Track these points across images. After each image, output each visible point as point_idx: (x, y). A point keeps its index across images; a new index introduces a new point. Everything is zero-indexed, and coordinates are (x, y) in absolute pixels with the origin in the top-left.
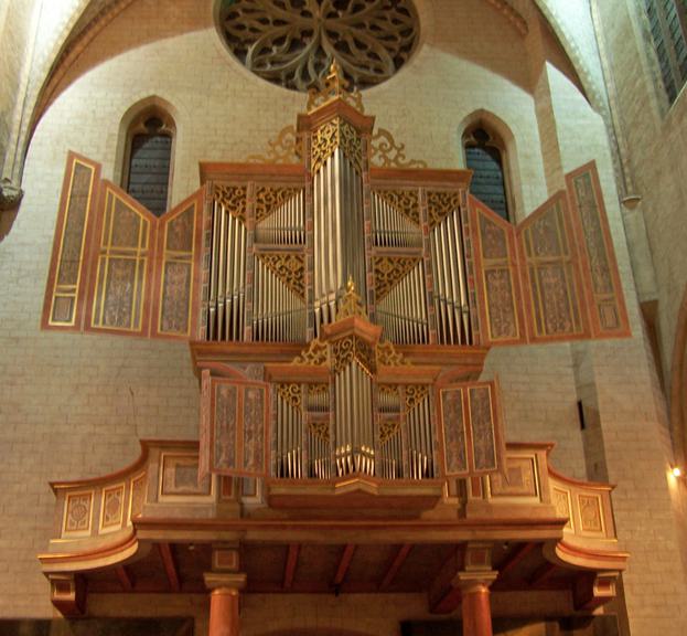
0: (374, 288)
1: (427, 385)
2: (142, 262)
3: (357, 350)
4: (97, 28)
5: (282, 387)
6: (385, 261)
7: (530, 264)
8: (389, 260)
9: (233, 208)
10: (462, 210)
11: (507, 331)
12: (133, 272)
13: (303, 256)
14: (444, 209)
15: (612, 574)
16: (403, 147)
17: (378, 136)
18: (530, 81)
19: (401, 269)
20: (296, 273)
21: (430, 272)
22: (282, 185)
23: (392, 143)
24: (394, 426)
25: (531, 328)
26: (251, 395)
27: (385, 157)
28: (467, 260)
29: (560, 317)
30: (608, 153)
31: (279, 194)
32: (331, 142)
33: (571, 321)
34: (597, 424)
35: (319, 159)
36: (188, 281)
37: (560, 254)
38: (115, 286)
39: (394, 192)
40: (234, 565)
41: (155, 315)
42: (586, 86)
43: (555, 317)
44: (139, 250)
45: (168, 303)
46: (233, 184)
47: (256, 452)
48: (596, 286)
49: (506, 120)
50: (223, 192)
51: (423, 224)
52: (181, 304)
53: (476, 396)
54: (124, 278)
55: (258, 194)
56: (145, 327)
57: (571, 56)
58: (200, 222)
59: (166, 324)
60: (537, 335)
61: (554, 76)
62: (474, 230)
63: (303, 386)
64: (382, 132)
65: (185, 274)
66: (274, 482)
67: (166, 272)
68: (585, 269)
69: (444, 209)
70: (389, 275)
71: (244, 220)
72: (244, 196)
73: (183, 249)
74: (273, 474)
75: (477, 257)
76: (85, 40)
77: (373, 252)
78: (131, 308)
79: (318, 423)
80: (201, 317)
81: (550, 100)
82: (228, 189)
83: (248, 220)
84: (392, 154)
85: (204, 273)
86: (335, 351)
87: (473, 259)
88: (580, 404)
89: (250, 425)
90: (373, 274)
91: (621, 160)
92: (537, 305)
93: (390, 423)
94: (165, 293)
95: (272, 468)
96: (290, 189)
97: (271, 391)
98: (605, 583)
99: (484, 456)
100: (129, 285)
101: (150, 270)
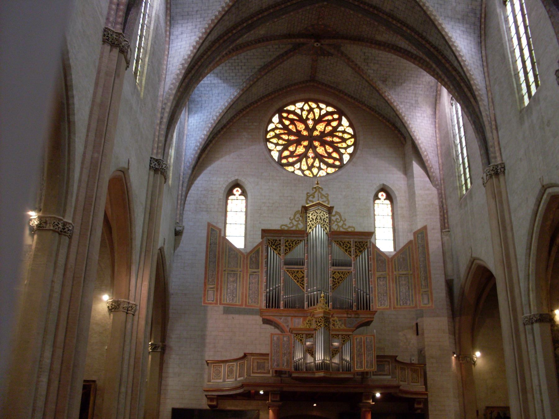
0: (332, 285)
1: (350, 335)
2: (240, 274)
3: (324, 323)
4: (211, 145)
5: (296, 335)
6: (337, 273)
7: (395, 275)
8: (338, 272)
9: (275, 250)
10: (369, 249)
11: (384, 304)
12: (237, 279)
13: (304, 271)
14: (362, 249)
15: (422, 400)
16: (345, 220)
17: (334, 216)
18: (407, 170)
19: (343, 276)
20: (301, 278)
23: (341, 219)
24: (337, 351)
25: (394, 303)
26: (285, 339)
27: (338, 226)
28: (370, 272)
29: (406, 299)
30: (438, 207)
31: (294, 243)
32: (316, 221)
33: (410, 301)
34: (423, 334)
35: (310, 228)
36: (258, 282)
37: (408, 271)
38: (230, 285)
39: (341, 241)
40: (278, 399)
41: (246, 297)
42: (430, 174)
43: (404, 299)
44: (239, 270)
45: (251, 292)
46: (276, 238)
47: (287, 361)
48: (422, 285)
49: (393, 189)
50: (271, 242)
51: (353, 256)
52: (256, 292)
53: (368, 340)
54: (233, 282)
55: (285, 243)
56: (242, 302)
57: (424, 159)
58: (262, 256)
59: (250, 301)
60: (396, 307)
61: (416, 168)
62: (374, 259)
63: (304, 335)
66: (293, 372)
67: (250, 279)
69: (362, 249)
70: (338, 279)
71: (280, 255)
72: (280, 244)
73: (256, 269)
74: (293, 369)
75: (374, 270)
76: (206, 152)
78: (236, 294)
79: (310, 349)
80: (264, 298)
81: (413, 181)
82: (273, 240)
83: (282, 255)
84: (340, 224)
86: (316, 322)
87: (372, 272)
88: (417, 324)
89: (285, 350)
90: (331, 279)
91: (444, 211)
92: (397, 293)
93: (336, 350)
94: (249, 287)
95: (293, 366)
96: (298, 241)
97: (292, 337)
98: (419, 403)
99: (369, 364)
100: (235, 285)
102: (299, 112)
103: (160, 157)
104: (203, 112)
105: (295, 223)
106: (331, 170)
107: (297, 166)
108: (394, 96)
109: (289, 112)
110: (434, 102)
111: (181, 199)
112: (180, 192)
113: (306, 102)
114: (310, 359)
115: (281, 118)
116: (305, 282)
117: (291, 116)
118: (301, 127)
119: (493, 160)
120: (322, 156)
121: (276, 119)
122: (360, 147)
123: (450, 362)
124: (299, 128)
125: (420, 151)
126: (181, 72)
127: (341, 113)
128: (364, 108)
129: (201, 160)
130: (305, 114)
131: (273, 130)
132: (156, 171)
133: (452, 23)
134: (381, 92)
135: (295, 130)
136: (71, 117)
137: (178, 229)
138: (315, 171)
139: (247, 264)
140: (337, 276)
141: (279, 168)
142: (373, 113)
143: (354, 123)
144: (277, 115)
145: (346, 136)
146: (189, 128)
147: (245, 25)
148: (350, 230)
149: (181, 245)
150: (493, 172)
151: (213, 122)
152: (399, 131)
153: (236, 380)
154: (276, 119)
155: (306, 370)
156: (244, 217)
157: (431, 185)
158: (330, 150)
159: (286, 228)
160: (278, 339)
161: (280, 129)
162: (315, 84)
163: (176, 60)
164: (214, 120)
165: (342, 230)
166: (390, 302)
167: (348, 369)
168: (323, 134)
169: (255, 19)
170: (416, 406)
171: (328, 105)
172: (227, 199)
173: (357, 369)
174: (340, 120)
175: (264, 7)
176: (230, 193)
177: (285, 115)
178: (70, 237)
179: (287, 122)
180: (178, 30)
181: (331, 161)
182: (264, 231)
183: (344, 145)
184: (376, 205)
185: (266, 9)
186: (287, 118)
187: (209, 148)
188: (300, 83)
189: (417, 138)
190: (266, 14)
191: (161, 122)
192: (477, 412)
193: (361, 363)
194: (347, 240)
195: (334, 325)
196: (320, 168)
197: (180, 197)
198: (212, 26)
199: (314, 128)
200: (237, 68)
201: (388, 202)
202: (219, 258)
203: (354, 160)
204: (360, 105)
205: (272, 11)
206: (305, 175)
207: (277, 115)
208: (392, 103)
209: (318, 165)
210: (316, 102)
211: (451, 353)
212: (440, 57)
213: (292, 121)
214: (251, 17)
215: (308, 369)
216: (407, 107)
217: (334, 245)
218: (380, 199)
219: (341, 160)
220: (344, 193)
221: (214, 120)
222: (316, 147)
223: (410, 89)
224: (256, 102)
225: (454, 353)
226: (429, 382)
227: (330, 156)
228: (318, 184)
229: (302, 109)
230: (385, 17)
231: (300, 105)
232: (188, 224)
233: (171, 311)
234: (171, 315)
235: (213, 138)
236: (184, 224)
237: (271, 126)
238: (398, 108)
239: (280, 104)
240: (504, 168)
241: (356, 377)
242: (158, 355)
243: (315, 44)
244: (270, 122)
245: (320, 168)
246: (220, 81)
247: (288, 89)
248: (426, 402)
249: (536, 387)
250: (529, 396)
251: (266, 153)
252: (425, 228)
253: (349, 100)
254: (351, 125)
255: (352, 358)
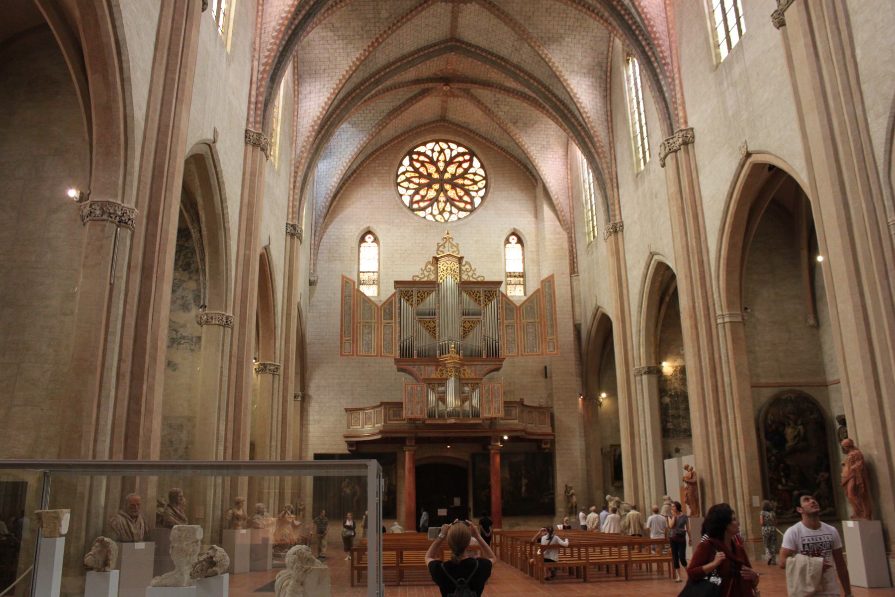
4: (342, 192)
9: (408, 300)
11: (512, 351)
17: (464, 266)
18: (537, 213)
21: (484, 326)
22: (426, 289)
26: (418, 388)
30: (567, 252)
34: (551, 377)
40: (413, 444)
42: (561, 218)
46: (408, 289)
49: (524, 233)
51: (482, 305)
58: (395, 307)
61: (547, 211)
62: (502, 308)
64: (467, 263)
65: (390, 330)
68: (545, 326)
74: (426, 417)
76: (337, 199)
77: (462, 318)
80: (398, 348)
84: (470, 274)
85: (398, 329)
98: (546, 443)
101: (378, 329)
102: (429, 153)
103: (295, 222)
104: (333, 157)
105: (426, 274)
106: (462, 214)
107: (429, 210)
108: (525, 138)
109: (419, 154)
110: (566, 142)
111: (314, 249)
112: (313, 242)
113: (437, 142)
114: (442, 407)
115: (411, 160)
116: (437, 331)
117: (422, 158)
118: (432, 169)
119: (612, 218)
120: (453, 200)
121: (406, 161)
122: (491, 190)
123: (577, 404)
124: (429, 171)
125: (551, 194)
126: (311, 135)
127: (472, 154)
128: (496, 148)
129: (332, 207)
130: (435, 155)
131: (404, 173)
132: (292, 235)
133: (578, 78)
134: (511, 134)
135: (425, 173)
136: (226, 225)
137: (312, 279)
138: (446, 215)
139: (381, 316)
140: (467, 325)
141: (409, 213)
142: (504, 154)
143: (485, 164)
144: (407, 158)
145: (477, 178)
146: (319, 174)
147: (372, 80)
148: (479, 279)
149: (316, 295)
150: (612, 230)
151: (342, 168)
152: (531, 173)
153: (374, 426)
154: (406, 161)
155: (439, 417)
156: (377, 264)
157: (561, 229)
158: (461, 193)
159: (418, 279)
160: (412, 388)
161: (411, 172)
162: (446, 124)
163: (305, 121)
164: (344, 166)
165: (472, 279)
166: (518, 350)
167: (476, 415)
168: (454, 176)
169: (382, 73)
170: (543, 446)
171: (459, 145)
172: (359, 246)
173: (486, 414)
174: (471, 160)
175: (391, 61)
176: (362, 240)
177: (415, 157)
178: (232, 329)
179: (417, 165)
180: (306, 89)
181: (462, 205)
182: (396, 283)
183: (476, 188)
184: (506, 249)
185: (393, 63)
186: (417, 161)
187: (339, 195)
188: (430, 123)
189: (548, 181)
190: (393, 67)
191: (294, 187)
192: (602, 449)
193: (489, 410)
194: (476, 290)
195: (464, 374)
196: (451, 213)
197: (312, 247)
198: (340, 86)
199: (445, 171)
200: (365, 112)
201: (519, 246)
202: (354, 311)
203: (485, 204)
204: (492, 146)
205: (399, 64)
206: (436, 221)
207: (407, 158)
208: (523, 146)
209: (449, 210)
210: (446, 142)
211: (578, 395)
212: (566, 112)
213: (423, 164)
214: (378, 72)
215: (441, 416)
216: (538, 148)
217: (464, 294)
218: (511, 243)
219: (472, 203)
220: (475, 239)
221: (344, 166)
222: (447, 191)
223: (541, 130)
224: (386, 145)
225: (581, 395)
226: (556, 423)
227: (461, 199)
228: (448, 234)
229: (433, 151)
230: (513, 69)
231: (430, 145)
232: (321, 274)
233: (308, 361)
234: (308, 365)
235: (344, 184)
236: (318, 273)
237: (402, 170)
238: (529, 150)
239: (411, 146)
240: (622, 226)
241: (485, 421)
242: (299, 404)
243: (445, 88)
244: (401, 164)
245: (451, 213)
246: (348, 126)
247: (419, 130)
248: (553, 442)
249: (642, 433)
250: (637, 440)
251: (397, 198)
252: (552, 276)
253: (480, 140)
254: (482, 167)
255: (481, 405)
